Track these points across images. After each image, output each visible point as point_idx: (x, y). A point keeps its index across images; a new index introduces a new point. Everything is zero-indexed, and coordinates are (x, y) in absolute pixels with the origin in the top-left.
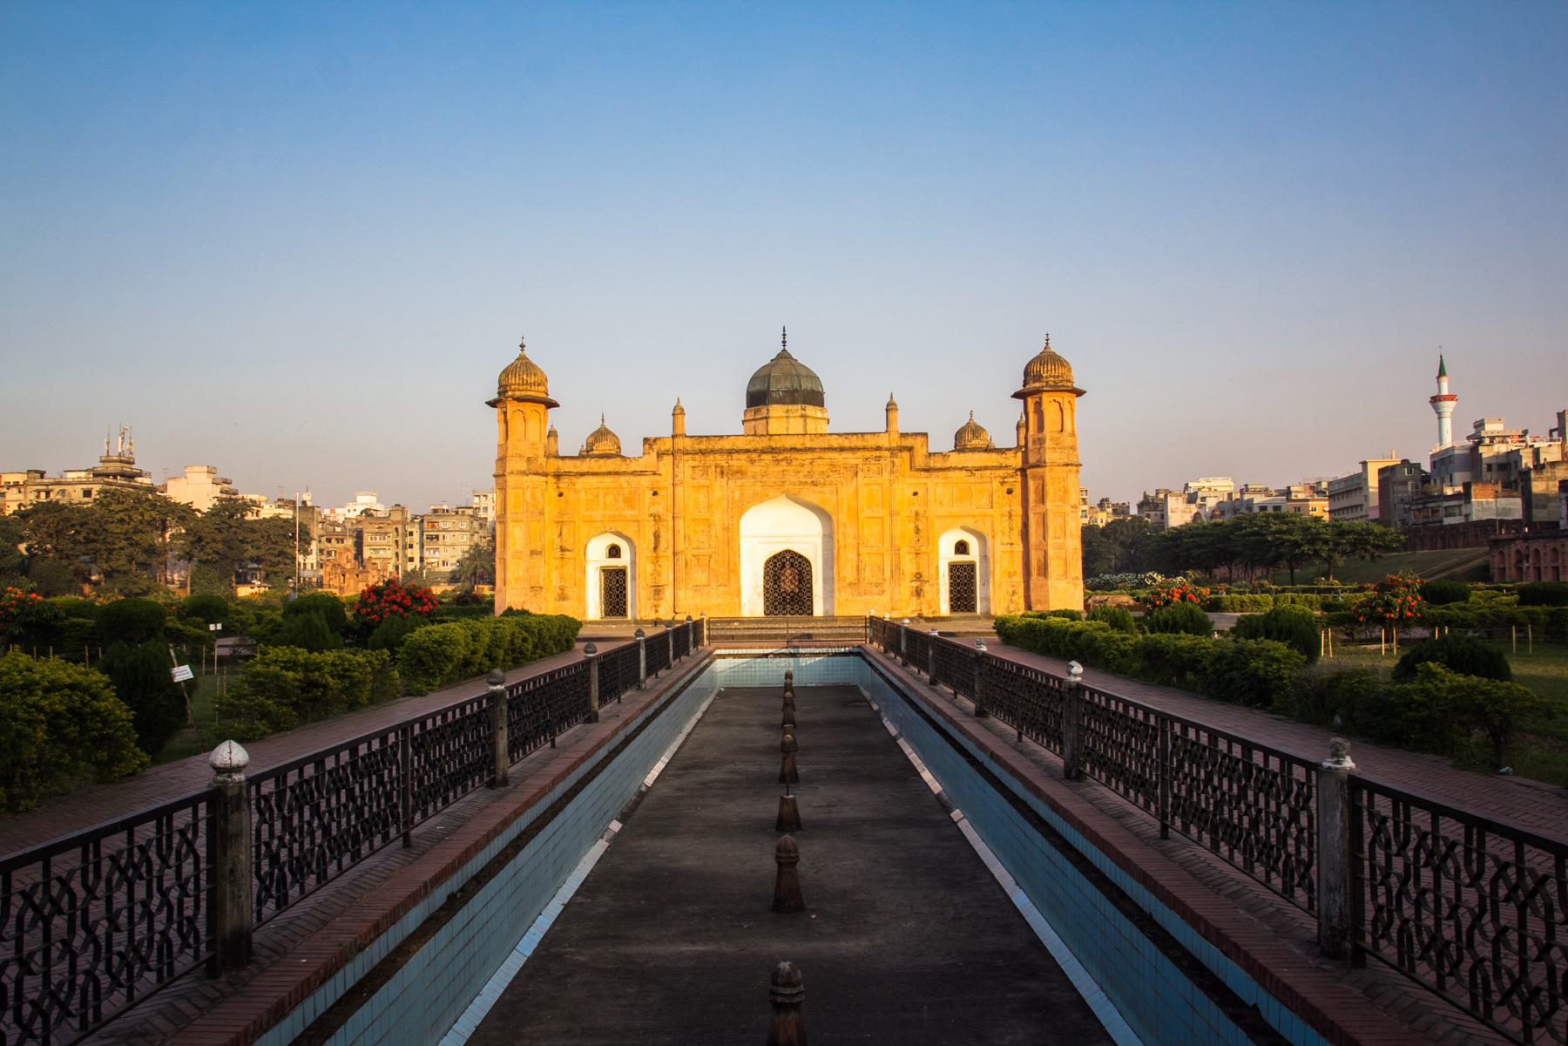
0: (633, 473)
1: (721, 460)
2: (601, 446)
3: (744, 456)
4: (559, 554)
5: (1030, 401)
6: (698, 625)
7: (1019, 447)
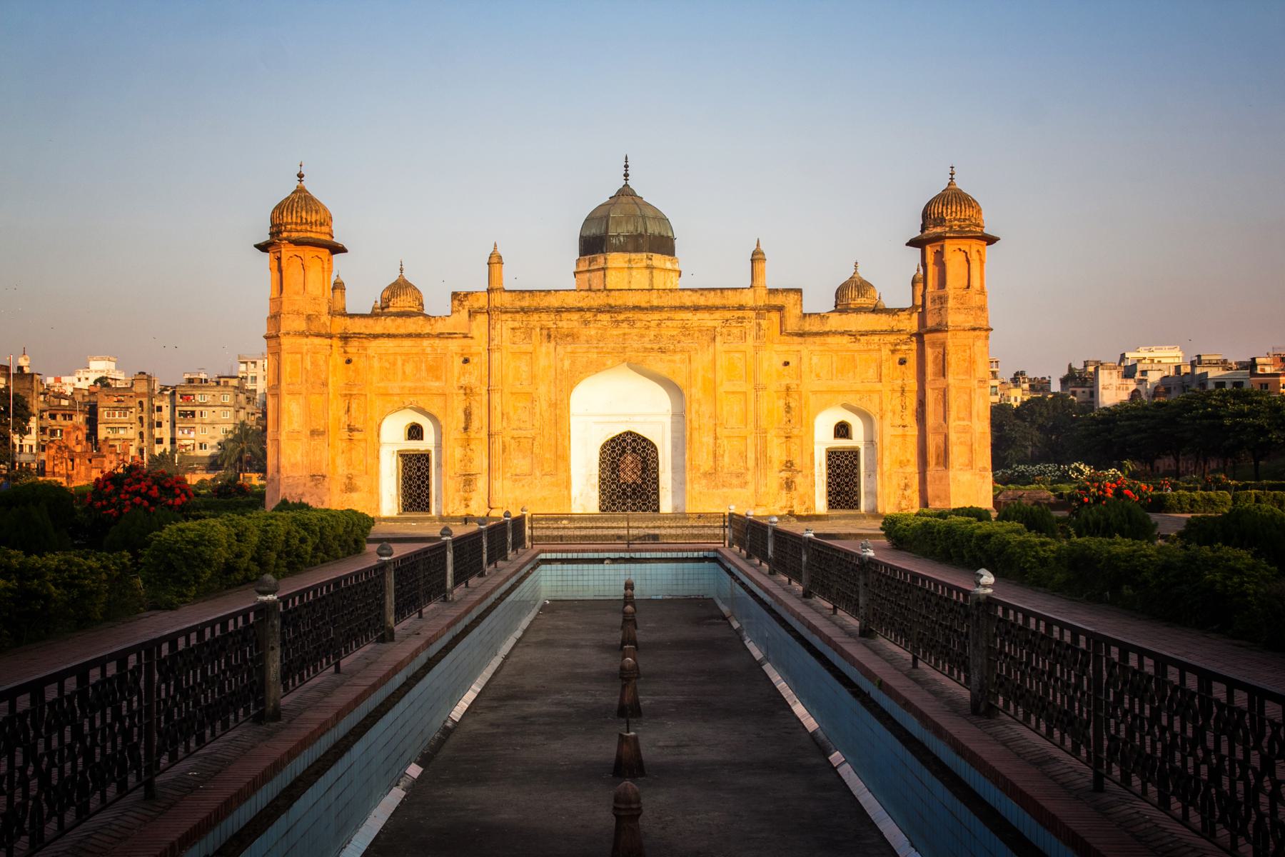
0: (439, 336)
1: (548, 320)
2: (399, 300)
3: (575, 316)
4: (345, 435)
5: (930, 250)
6: (518, 523)
7: (914, 307)
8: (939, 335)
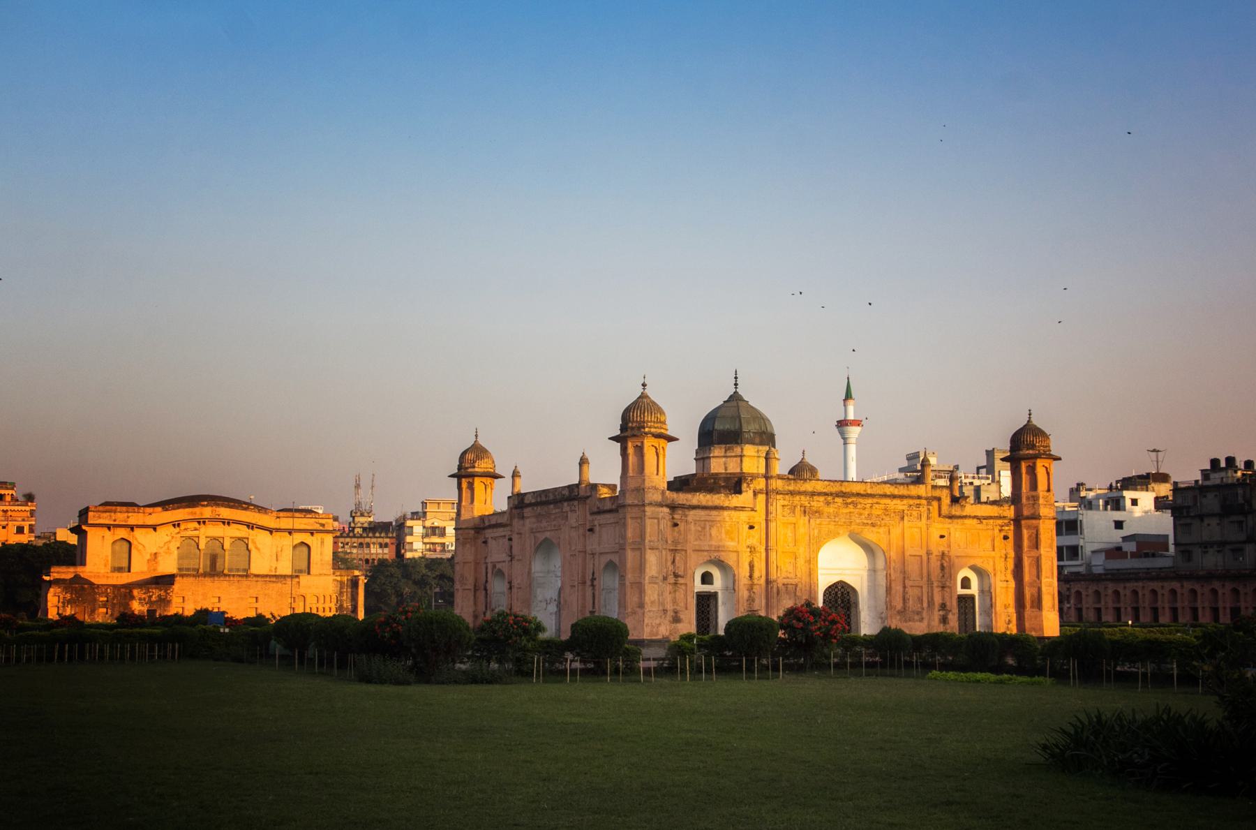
0: (735, 508)
1: (804, 500)
3: (822, 499)
8: (1034, 521)
